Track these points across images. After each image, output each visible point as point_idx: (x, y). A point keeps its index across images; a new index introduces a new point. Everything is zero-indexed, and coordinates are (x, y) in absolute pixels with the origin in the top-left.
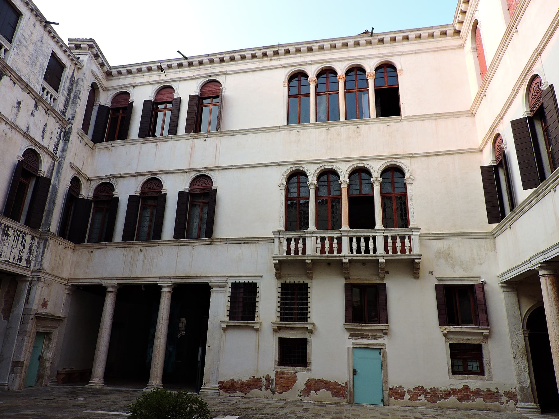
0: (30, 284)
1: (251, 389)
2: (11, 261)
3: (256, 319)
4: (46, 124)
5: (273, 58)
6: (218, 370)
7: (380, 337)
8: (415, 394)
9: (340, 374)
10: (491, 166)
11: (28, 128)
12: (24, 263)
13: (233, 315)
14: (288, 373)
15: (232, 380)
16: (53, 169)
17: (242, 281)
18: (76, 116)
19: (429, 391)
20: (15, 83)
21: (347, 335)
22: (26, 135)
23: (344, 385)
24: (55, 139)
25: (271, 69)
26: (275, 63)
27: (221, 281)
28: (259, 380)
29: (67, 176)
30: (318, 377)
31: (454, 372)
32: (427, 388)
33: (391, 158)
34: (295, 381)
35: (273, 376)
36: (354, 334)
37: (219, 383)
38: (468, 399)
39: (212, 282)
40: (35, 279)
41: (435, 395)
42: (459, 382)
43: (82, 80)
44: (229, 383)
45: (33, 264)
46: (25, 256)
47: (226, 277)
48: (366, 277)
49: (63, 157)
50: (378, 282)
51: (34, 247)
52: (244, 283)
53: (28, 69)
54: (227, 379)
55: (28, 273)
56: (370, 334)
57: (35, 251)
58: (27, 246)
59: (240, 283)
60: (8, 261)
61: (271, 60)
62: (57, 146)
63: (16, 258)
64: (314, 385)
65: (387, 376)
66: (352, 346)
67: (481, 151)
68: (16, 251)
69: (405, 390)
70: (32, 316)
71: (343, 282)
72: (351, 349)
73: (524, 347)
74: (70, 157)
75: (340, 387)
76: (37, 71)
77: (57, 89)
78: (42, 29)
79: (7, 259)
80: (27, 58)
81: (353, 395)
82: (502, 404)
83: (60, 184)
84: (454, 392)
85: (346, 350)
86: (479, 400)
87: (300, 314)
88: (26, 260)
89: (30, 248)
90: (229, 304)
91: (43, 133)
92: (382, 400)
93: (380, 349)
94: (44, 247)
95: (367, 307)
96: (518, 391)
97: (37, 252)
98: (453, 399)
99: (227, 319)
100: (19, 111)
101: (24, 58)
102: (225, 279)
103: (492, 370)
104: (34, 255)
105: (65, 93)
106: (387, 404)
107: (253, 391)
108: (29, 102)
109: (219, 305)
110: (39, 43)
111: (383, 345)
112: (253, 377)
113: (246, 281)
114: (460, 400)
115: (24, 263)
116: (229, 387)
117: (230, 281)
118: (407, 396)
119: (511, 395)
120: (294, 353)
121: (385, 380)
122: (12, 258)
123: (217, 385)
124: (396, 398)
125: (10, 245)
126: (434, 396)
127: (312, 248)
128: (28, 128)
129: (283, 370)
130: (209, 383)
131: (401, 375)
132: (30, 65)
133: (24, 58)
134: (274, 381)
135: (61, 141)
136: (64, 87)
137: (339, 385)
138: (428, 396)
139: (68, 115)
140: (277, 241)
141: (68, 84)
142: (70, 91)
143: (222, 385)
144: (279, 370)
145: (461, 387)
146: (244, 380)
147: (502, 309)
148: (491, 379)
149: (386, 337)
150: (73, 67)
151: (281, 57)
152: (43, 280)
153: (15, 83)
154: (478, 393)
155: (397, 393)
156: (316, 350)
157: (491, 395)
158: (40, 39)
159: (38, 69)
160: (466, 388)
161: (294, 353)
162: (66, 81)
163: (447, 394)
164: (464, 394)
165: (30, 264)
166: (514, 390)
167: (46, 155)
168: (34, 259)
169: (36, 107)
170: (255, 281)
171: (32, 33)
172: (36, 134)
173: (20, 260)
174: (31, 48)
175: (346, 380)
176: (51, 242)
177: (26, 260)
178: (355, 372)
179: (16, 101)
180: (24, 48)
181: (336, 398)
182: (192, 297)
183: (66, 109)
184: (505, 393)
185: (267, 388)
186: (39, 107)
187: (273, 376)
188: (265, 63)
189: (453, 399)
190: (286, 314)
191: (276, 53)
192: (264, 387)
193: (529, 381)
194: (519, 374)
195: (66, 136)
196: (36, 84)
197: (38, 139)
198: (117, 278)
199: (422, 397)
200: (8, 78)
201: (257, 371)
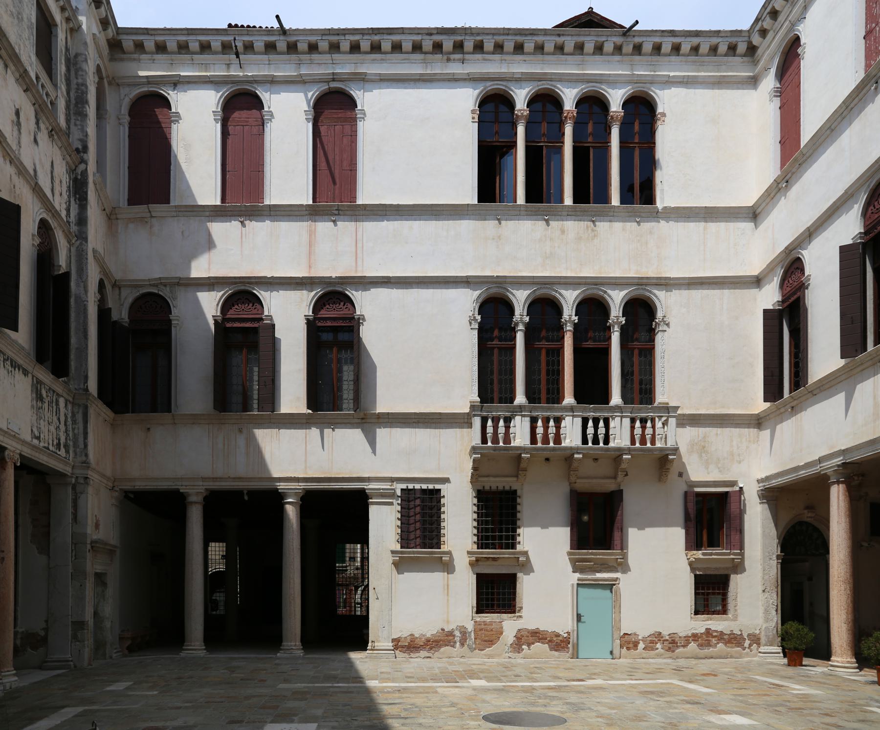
0: (74, 488)
1: (440, 647)
5: (452, 56)
6: (390, 622)
8: (652, 642)
9: (560, 622)
13: (405, 540)
14: (491, 623)
15: (412, 635)
17: (417, 486)
19: (667, 638)
23: (565, 635)
25: (449, 80)
26: (455, 68)
28: (451, 634)
29: (93, 275)
30: (532, 627)
31: (697, 613)
32: (665, 633)
34: (502, 633)
35: (470, 626)
37: (393, 640)
38: (709, 645)
40: (82, 481)
41: (673, 642)
42: (702, 624)
44: (409, 640)
47: (392, 480)
52: (424, 491)
54: (405, 634)
59: (414, 490)
60: (48, 449)
61: (448, 60)
64: (528, 638)
69: (640, 638)
70: (89, 547)
72: (575, 586)
73: (775, 580)
75: (560, 638)
81: (576, 647)
82: (744, 649)
84: (695, 637)
85: (570, 588)
86: (721, 646)
87: (507, 538)
92: (611, 653)
93: (610, 586)
95: (597, 526)
96: (763, 633)
97: (73, 429)
98: (693, 646)
99: (398, 547)
103: (737, 608)
106: (618, 656)
107: (442, 649)
111: (617, 579)
112: (443, 630)
113: (424, 487)
114: (700, 646)
116: (408, 646)
117: (399, 487)
118: (641, 646)
119: (755, 640)
120: (497, 592)
121: (616, 625)
123: (391, 644)
124: (628, 649)
126: (673, 643)
127: (520, 433)
129: (485, 619)
130: (379, 641)
131: (637, 620)
134: (473, 634)
137: (558, 635)
138: (666, 643)
140: (477, 422)
143: (397, 644)
144: (478, 619)
145: (703, 630)
146: (428, 635)
147: (759, 530)
148: (735, 618)
151: (467, 56)
154: (721, 636)
155: (629, 642)
156: (528, 588)
157: (734, 640)
160: (708, 632)
161: (497, 592)
163: (687, 640)
164: (706, 639)
166: (757, 632)
170: (437, 487)
175: (569, 629)
178: (579, 618)
181: (556, 653)
182: (339, 512)
184: (749, 635)
185: (462, 645)
187: (470, 626)
188: (438, 67)
189: (693, 646)
190: (487, 538)
191: (459, 47)
192: (458, 644)
193: (775, 619)
194: (766, 611)
198: (204, 479)
199: (659, 646)
201: (448, 622)
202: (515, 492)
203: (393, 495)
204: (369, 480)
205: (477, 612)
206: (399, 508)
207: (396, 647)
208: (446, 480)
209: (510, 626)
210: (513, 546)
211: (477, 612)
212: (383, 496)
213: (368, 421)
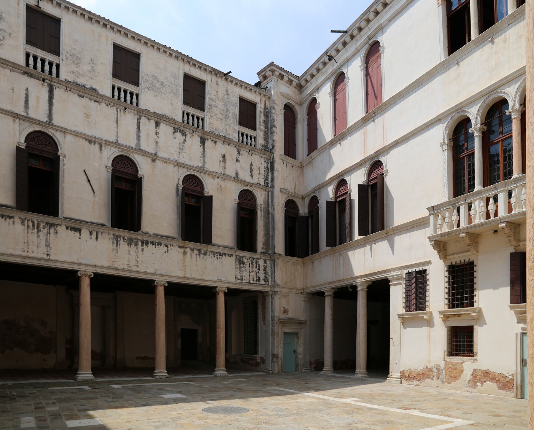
2: (251, 282)
4: (251, 164)
11: (237, 173)
12: (262, 282)
16: (268, 199)
18: (275, 145)
20: (216, 142)
22: (236, 179)
24: (263, 172)
43: (274, 108)
45: (270, 282)
46: (262, 276)
49: (273, 187)
51: (268, 267)
53: (223, 124)
55: (267, 289)
57: (269, 271)
58: (262, 268)
62: (266, 178)
63: (255, 279)
68: (253, 274)
74: (278, 184)
76: (231, 122)
77: (254, 129)
78: (225, 83)
79: (248, 281)
80: (220, 116)
83: (275, 211)
88: (264, 279)
89: (265, 270)
91: (251, 172)
94: (274, 267)
100: (225, 163)
101: (217, 116)
104: (270, 274)
105: (263, 128)
108: (231, 151)
110: (226, 97)
115: (262, 282)
122: (251, 280)
125: (248, 270)
128: (237, 173)
132: (224, 120)
133: (217, 116)
135: (269, 172)
136: (260, 123)
139: (270, 146)
141: (263, 118)
142: (266, 123)
150: (263, 99)
152: (279, 293)
153: (216, 142)
158: (225, 93)
159: (232, 119)
162: (260, 117)
165: (268, 281)
167: (259, 190)
168: (270, 277)
169: (239, 153)
171: (217, 92)
172: (245, 176)
173: (259, 280)
174: (220, 105)
176: (280, 263)
177: (264, 279)
179: (221, 156)
180: (215, 108)
183: (267, 142)
186: (242, 152)
195: (271, 167)
196: (234, 133)
197: (248, 179)
200: (210, 140)
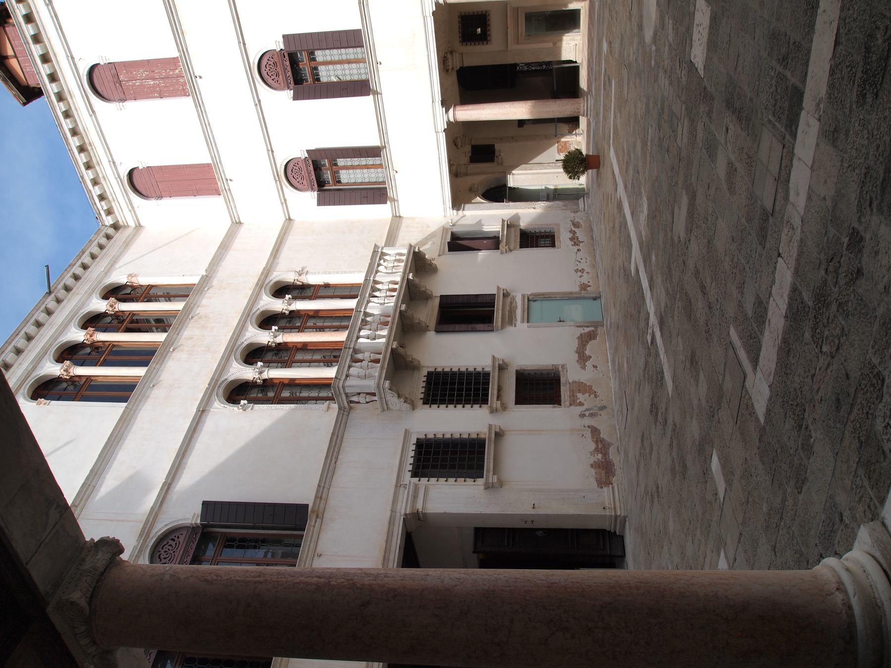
3: (482, 436)
7: (513, 298)
10: (319, 196)
21: (510, 329)
27: (404, 495)
33: (260, 286)
36: (510, 320)
39: (403, 508)
47: (398, 485)
48: (428, 314)
50: (437, 301)
56: (508, 308)
65: (564, 293)
66: (526, 324)
67: (290, 219)
71: (431, 335)
90: (451, 480)
92: (595, 299)
93: (530, 300)
102: (402, 489)
109: (452, 498)
111: (523, 296)
116: (605, 471)
120: (539, 387)
123: (605, 489)
129: (567, 398)
144: (568, 403)
148: (558, 225)
149: (513, 294)
161: (539, 387)
187: (578, 410)
202: (430, 374)
203: (416, 488)
204: (393, 511)
205: (560, 404)
206: (433, 480)
207: (608, 483)
208: (407, 433)
209: (572, 374)
210: (486, 375)
211: (560, 404)
212: (415, 497)
213: (321, 510)
